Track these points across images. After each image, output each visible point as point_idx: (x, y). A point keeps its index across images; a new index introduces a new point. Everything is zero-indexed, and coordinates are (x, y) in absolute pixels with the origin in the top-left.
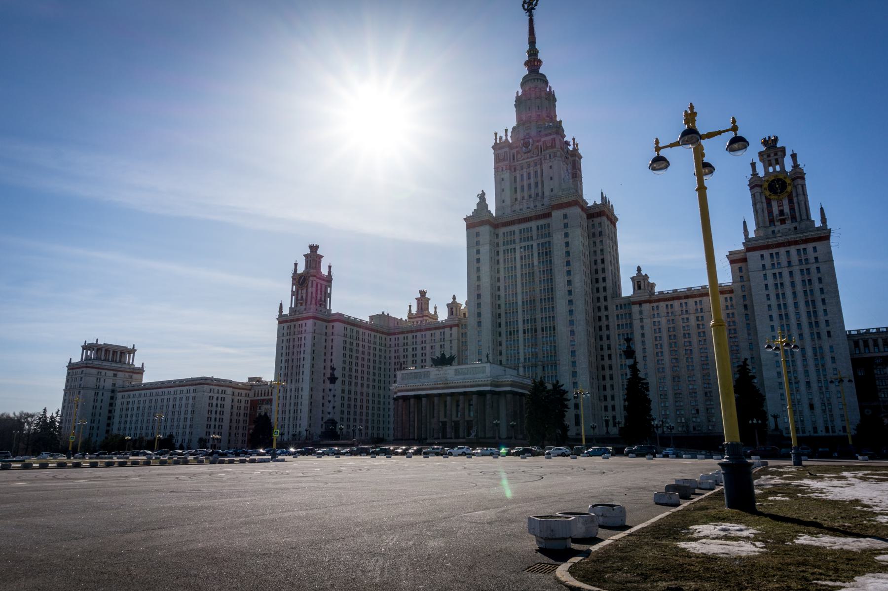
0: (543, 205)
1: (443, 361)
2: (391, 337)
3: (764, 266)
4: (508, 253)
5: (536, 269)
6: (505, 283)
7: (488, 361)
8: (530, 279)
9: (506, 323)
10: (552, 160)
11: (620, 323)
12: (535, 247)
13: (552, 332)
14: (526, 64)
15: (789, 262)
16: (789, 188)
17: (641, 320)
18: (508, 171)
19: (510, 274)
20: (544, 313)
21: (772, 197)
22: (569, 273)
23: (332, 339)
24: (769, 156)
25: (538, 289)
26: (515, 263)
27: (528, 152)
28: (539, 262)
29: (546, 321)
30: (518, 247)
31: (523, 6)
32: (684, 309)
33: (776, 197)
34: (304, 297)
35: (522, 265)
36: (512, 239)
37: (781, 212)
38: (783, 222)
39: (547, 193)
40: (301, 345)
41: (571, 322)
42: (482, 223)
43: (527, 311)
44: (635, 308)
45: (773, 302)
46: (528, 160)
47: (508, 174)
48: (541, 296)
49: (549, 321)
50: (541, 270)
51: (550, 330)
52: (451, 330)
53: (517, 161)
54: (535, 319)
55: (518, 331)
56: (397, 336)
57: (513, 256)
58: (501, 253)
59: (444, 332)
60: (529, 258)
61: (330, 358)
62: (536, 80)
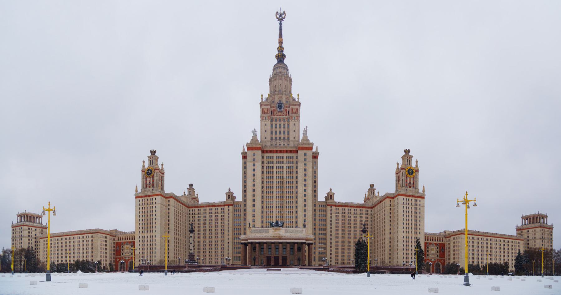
0: (288, 145)
4: (269, 168)
5: (285, 180)
6: (267, 185)
8: (281, 185)
9: (266, 207)
10: (295, 121)
13: (292, 214)
14: (277, 57)
18: (270, 120)
19: (270, 181)
20: (288, 204)
22: (305, 185)
23: (169, 208)
25: (285, 191)
26: (273, 175)
27: (281, 112)
28: (287, 177)
29: (289, 208)
32: (361, 212)
35: (277, 177)
36: (272, 161)
39: (291, 139)
40: (153, 211)
41: (305, 211)
46: (280, 117)
47: (269, 122)
48: (287, 195)
49: (291, 208)
50: (288, 181)
51: (290, 213)
53: (274, 116)
54: (283, 206)
55: (273, 211)
57: (272, 171)
60: (281, 173)
61: (168, 219)
62: (284, 69)
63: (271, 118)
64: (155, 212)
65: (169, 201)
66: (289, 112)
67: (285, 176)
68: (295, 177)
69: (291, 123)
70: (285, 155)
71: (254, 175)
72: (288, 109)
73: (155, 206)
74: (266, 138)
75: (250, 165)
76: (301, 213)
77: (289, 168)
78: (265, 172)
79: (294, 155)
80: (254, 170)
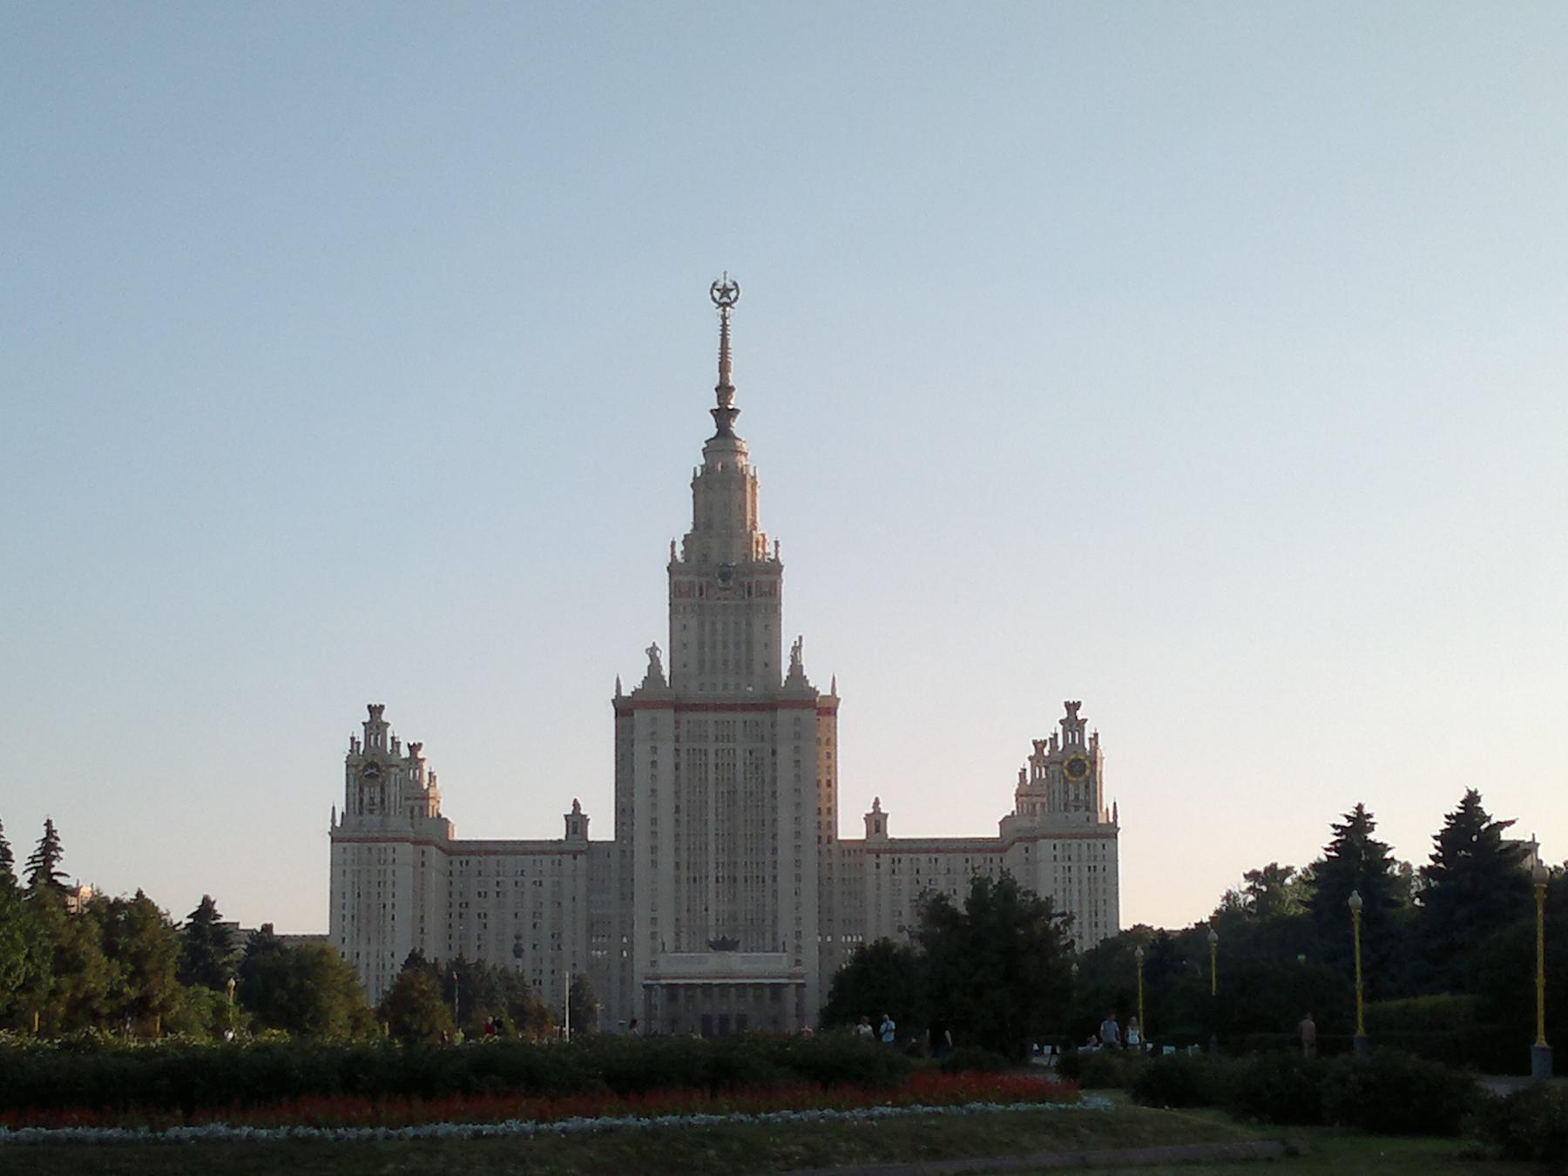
1: (723, 945)
2: (453, 858)
3: (1055, 857)
5: (740, 788)
7: (784, 951)
11: (846, 877)
12: (739, 752)
15: (1079, 856)
16: (1088, 772)
21: (1070, 778)
24: (1071, 725)
30: (711, 751)
31: (712, 293)
33: (1074, 779)
34: (377, 800)
37: (1077, 796)
38: (1077, 808)
41: (798, 878)
43: (723, 850)
50: (748, 790)
52: (575, 858)
54: (736, 863)
56: (464, 858)
58: (683, 754)
59: (560, 861)
63: (700, 606)
64: (394, 886)
65: (423, 853)
66: (750, 588)
67: (740, 777)
70: (740, 717)
72: (746, 580)
73: (394, 871)
74: (685, 666)
76: (785, 884)
77: (751, 753)
78: (683, 766)
80: (654, 764)
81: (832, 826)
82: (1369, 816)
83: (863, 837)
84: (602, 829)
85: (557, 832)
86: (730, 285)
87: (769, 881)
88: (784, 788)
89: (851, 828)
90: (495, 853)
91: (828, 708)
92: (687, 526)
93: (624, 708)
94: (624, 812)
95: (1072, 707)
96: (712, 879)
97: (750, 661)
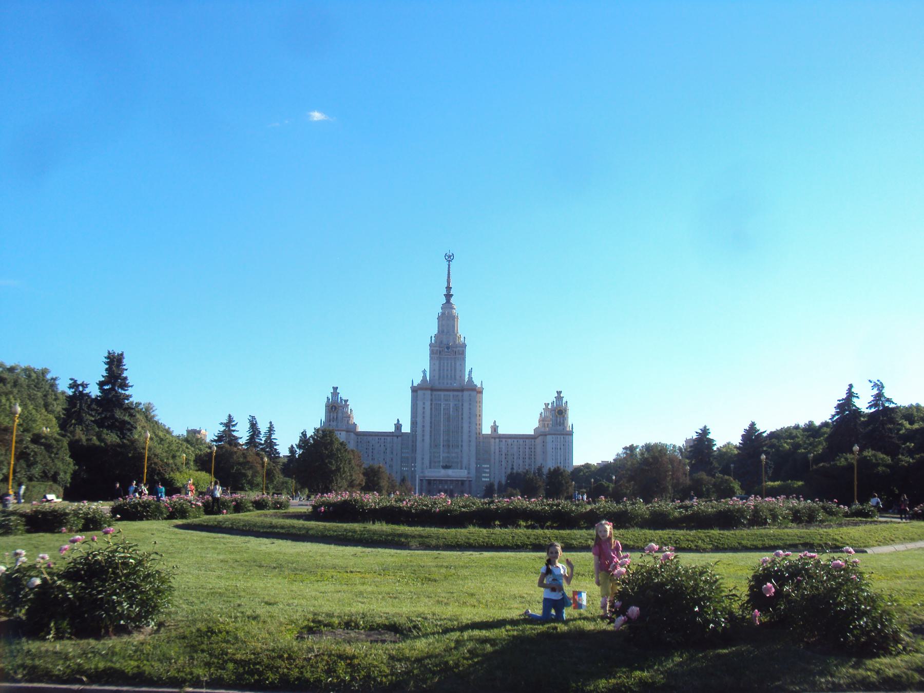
1: (446, 467)
12: (451, 406)
17: (495, 446)
22: (470, 423)
30: (442, 404)
34: (335, 417)
37: (560, 421)
39: (458, 377)
42: (426, 389)
44: (493, 440)
45: (554, 454)
58: (433, 405)
67: (451, 413)
68: (460, 413)
69: (458, 363)
70: (451, 393)
71: (424, 412)
75: (420, 404)
76: (465, 448)
79: (460, 394)
80: (424, 408)
81: (481, 429)
82: (708, 429)
83: (489, 432)
84: (406, 428)
85: (392, 429)
86: (451, 254)
87: (460, 446)
88: (465, 416)
89: (486, 430)
90: (372, 436)
91: (480, 392)
92: (436, 332)
93: (414, 390)
94: (414, 424)
95: (559, 393)
96: (441, 446)
97: (455, 376)
